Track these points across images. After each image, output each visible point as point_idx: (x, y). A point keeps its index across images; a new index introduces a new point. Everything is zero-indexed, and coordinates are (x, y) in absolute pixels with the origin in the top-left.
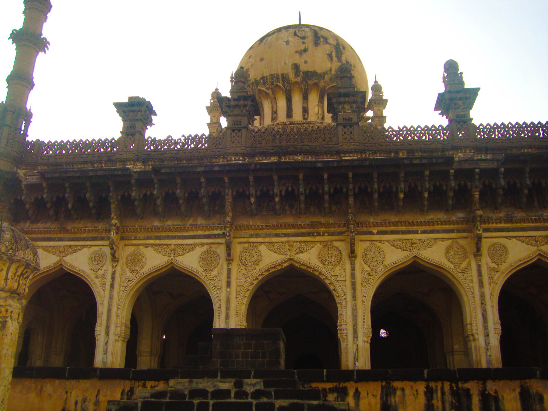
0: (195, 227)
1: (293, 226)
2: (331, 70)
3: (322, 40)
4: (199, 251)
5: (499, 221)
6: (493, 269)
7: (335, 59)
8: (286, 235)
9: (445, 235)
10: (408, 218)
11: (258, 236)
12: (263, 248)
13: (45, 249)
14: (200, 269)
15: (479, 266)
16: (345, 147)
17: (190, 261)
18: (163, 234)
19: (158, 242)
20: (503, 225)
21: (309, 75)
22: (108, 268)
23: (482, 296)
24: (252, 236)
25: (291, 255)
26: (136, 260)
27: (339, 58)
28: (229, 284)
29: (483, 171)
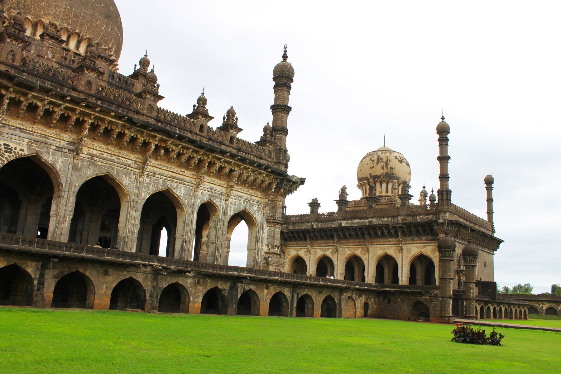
0: (329, 243)
4: (331, 250)
5: (410, 241)
7: (385, 168)
10: (384, 240)
12: (346, 249)
13: (293, 249)
16: (369, 216)
17: (328, 253)
20: (411, 242)
21: (375, 177)
22: (309, 255)
23: (402, 265)
25: (353, 251)
26: (315, 253)
27: (387, 168)
29: (400, 227)
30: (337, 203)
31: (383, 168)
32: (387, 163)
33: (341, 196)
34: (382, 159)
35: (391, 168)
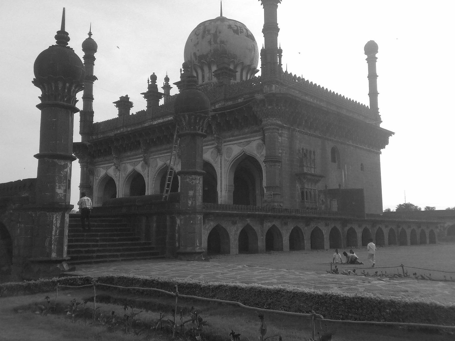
1: (165, 149)
2: (211, 51)
3: (207, 32)
4: (141, 163)
6: (226, 160)
7: (212, 43)
8: (163, 153)
9: (211, 146)
11: (156, 155)
12: (158, 159)
14: (141, 170)
15: (221, 160)
17: (139, 168)
18: (131, 158)
19: (130, 161)
23: (221, 173)
24: (154, 155)
28: (148, 176)
30: (145, 97)
31: (210, 42)
32: (215, 36)
33: (150, 87)
34: (209, 31)
35: (222, 42)
